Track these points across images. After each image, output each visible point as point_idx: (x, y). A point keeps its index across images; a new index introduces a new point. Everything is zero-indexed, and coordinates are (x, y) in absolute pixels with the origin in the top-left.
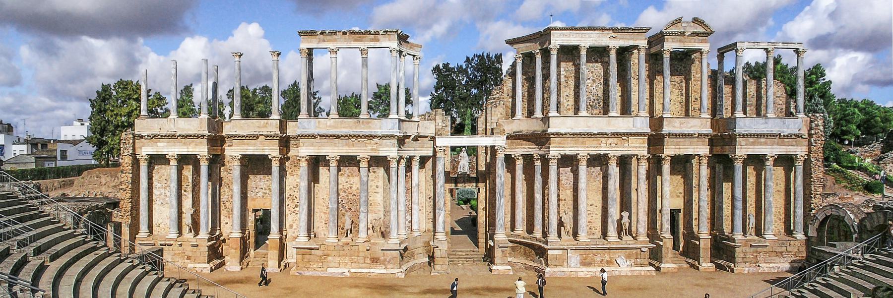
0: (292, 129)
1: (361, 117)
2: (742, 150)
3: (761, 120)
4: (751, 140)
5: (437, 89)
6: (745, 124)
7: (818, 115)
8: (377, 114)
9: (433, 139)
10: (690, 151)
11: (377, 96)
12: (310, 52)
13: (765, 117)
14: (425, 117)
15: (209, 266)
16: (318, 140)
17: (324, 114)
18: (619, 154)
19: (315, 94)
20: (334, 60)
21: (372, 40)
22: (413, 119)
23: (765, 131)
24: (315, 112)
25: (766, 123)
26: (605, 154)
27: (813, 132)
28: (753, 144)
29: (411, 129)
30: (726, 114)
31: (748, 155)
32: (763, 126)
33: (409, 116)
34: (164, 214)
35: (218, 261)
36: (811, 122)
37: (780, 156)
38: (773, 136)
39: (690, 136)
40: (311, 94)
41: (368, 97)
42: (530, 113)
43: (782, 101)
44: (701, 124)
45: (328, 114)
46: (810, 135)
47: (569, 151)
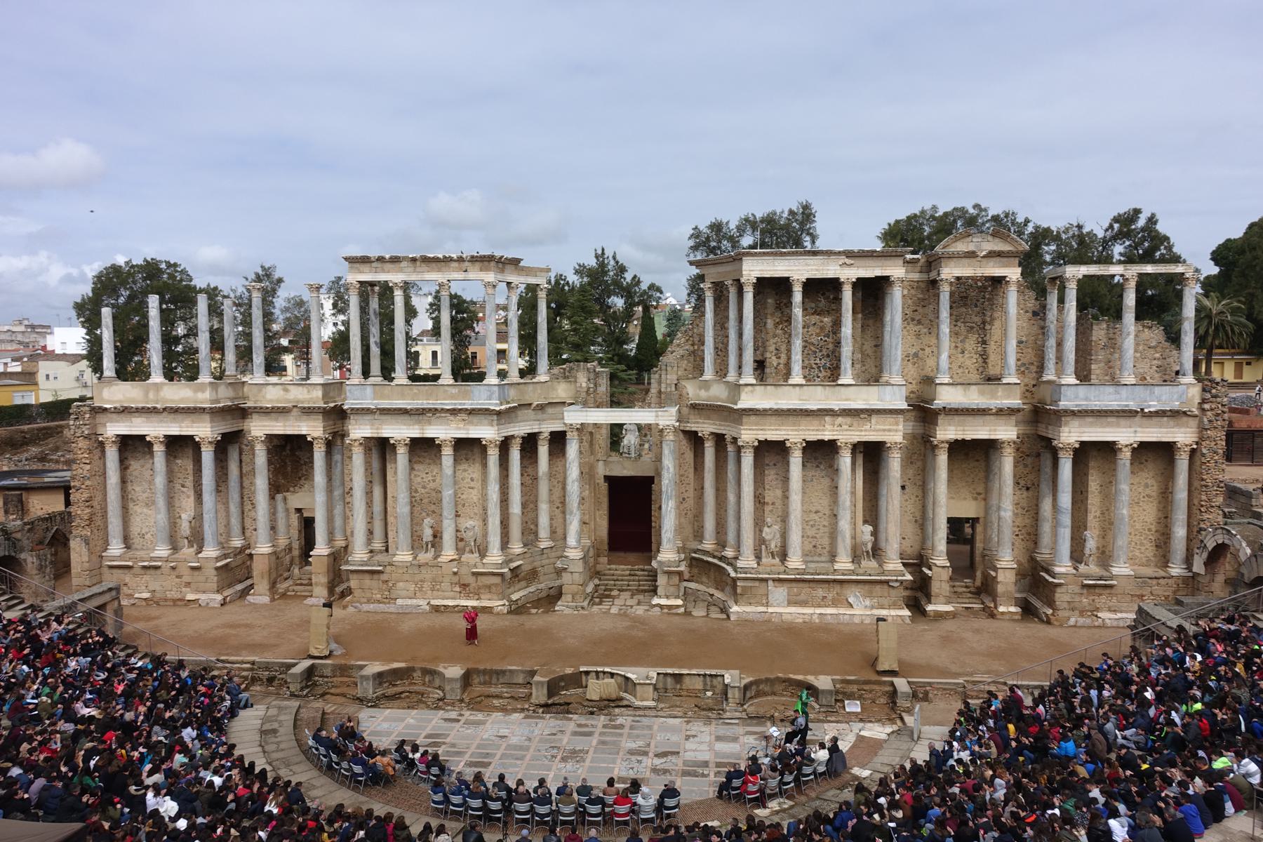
13: (1118, 384)
15: (219, 597)
18: (856, 439)
23: (1114, 404)
26: (830, 441)
28: (1091, 425)
30: (1050, 376)
31: (1082, 443)
32: (1112, 397)
34: (150, 519)
35: (239, 587)
42: (721, 371)
47: (773, 435)
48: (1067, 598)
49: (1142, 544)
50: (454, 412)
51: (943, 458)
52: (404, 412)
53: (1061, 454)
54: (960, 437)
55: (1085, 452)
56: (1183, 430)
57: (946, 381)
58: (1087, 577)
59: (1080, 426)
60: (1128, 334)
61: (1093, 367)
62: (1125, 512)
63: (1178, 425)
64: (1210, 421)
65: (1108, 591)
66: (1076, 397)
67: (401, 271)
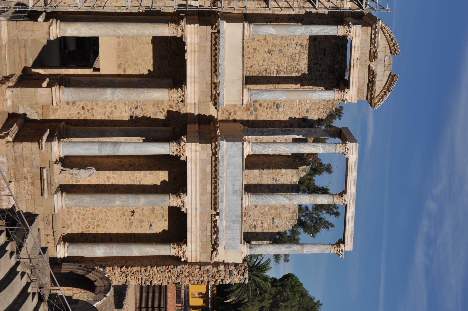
2: (194, 154)
3: (239, 186)
4: (209, 168)
6: (232, 153)
7: (246, 275)
10: (192, 70)
23: (222, 189)
25: (234, 192)
27: (221, 267)
28: (203, 171)
36: (236, 265)
37: (184, 216)
38: (215, 205)
39: (215, 68)
43: (266, 227)
44: (234, 98)
46: (217, 264)
48: (27, 154)
49: (84, 220)
51: (165, 30)
53: (174, 145)
54: (188, 47)
55: (177, 168)
56: (198, 249)
57: (247, 33)
58: (51, 171)
59: (202, 161)
60: (290, 199)
61: (256, 171)
62: (118, 203)
63: (203, 246)
64: (208, 271)
65: (38, 192)
66: (231, 156)
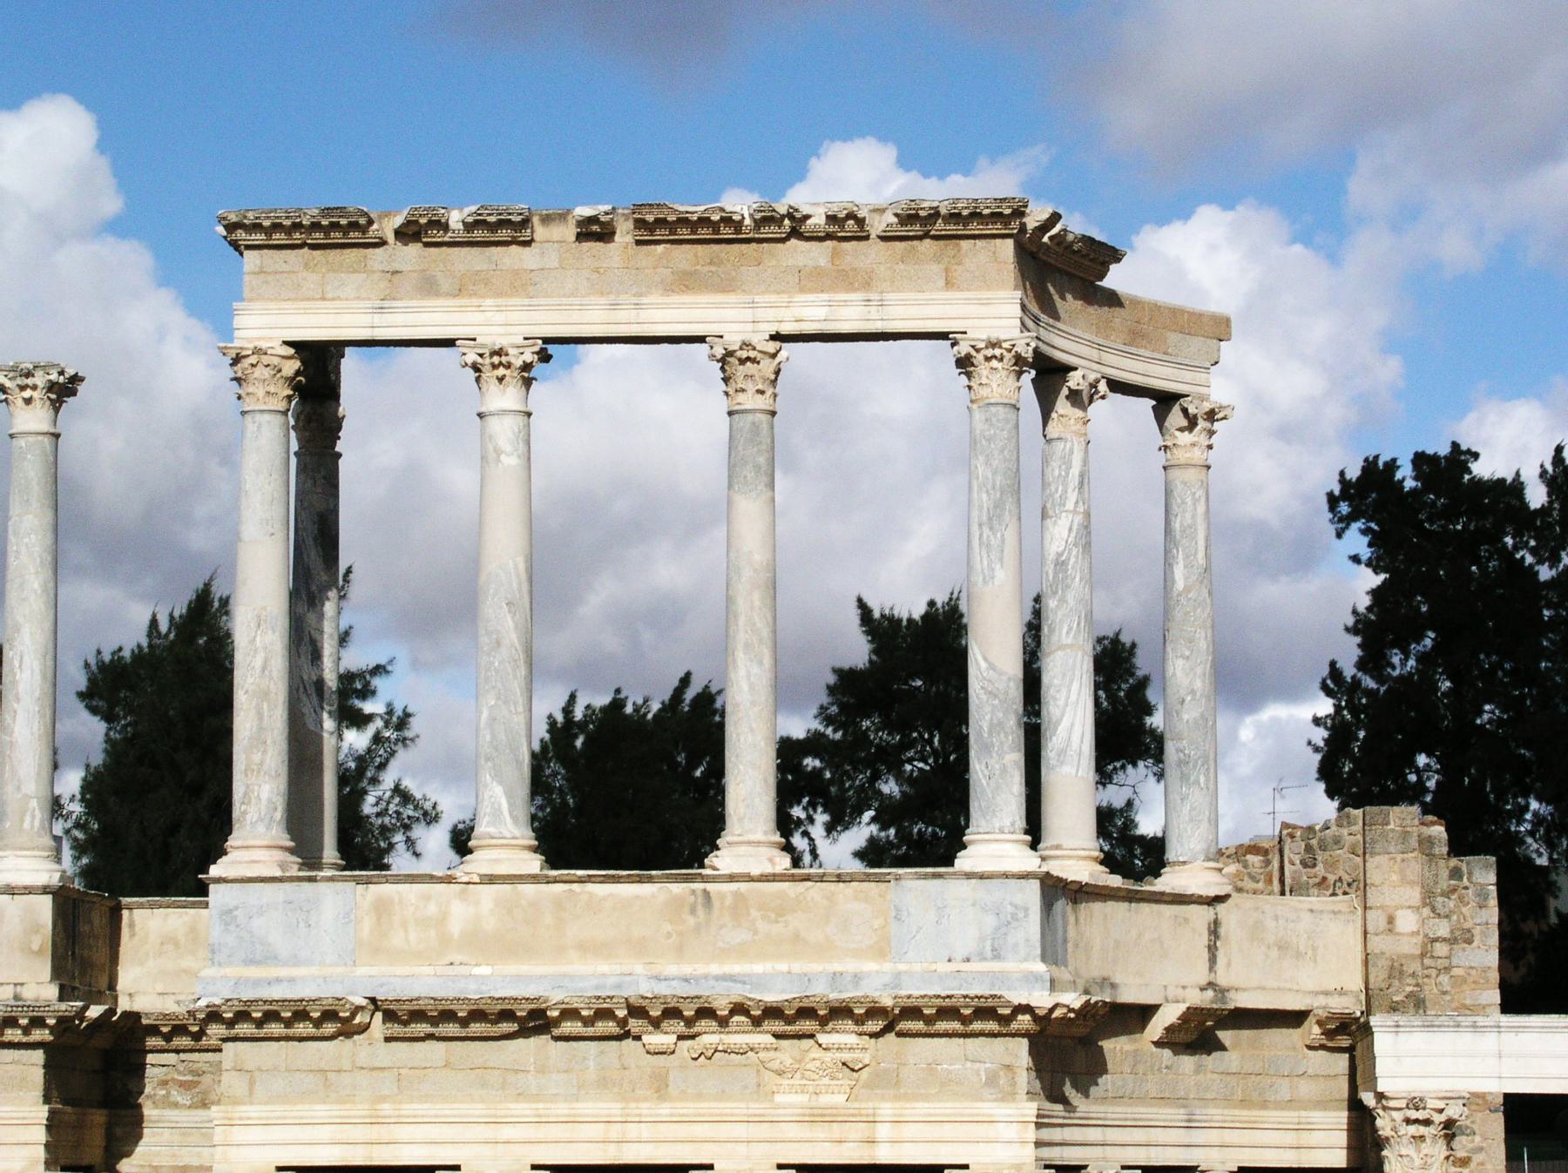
0: (164, 958)
1: (723, 860)
5: (1378, 628)
8: (862, 832)
9: (1349, 1035)
11: (852, 692)
12: (317, 373)
14: (1279, 863)
16: (372, 1046)
17: (434, 840)
19: (355, 686)
20: (504, 431)
21: (810, 281)
22: (1168, 881)
24: (355, 834)
29: (1152, 957)
33: (1133, 855)
40: (327, 695)
41: (783, 694)
45: (461, 842)
50: (799, 1018)
52: (535, 1021)
67: (520, 284)
